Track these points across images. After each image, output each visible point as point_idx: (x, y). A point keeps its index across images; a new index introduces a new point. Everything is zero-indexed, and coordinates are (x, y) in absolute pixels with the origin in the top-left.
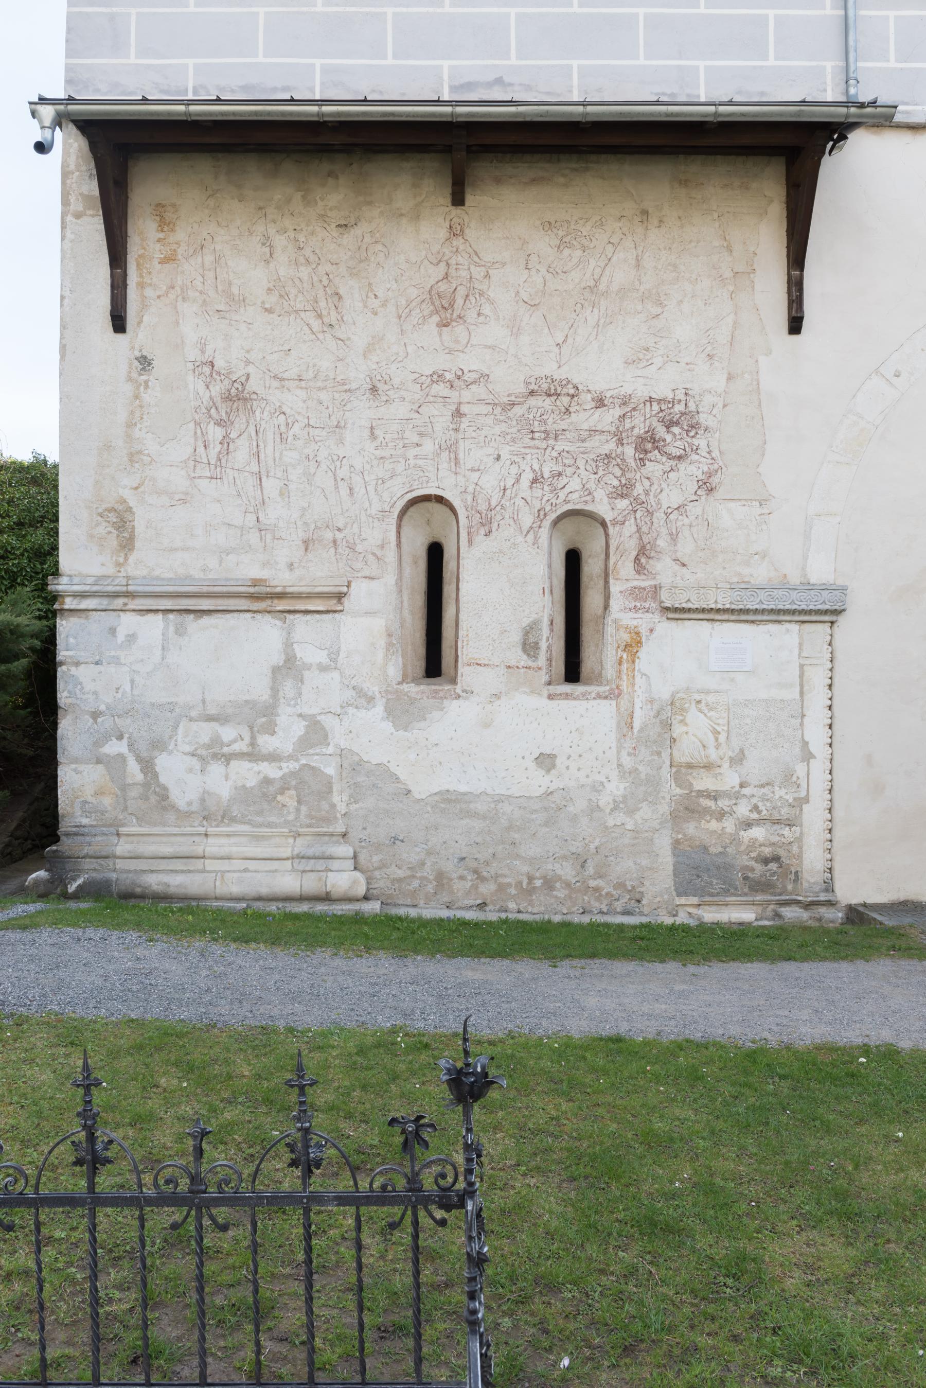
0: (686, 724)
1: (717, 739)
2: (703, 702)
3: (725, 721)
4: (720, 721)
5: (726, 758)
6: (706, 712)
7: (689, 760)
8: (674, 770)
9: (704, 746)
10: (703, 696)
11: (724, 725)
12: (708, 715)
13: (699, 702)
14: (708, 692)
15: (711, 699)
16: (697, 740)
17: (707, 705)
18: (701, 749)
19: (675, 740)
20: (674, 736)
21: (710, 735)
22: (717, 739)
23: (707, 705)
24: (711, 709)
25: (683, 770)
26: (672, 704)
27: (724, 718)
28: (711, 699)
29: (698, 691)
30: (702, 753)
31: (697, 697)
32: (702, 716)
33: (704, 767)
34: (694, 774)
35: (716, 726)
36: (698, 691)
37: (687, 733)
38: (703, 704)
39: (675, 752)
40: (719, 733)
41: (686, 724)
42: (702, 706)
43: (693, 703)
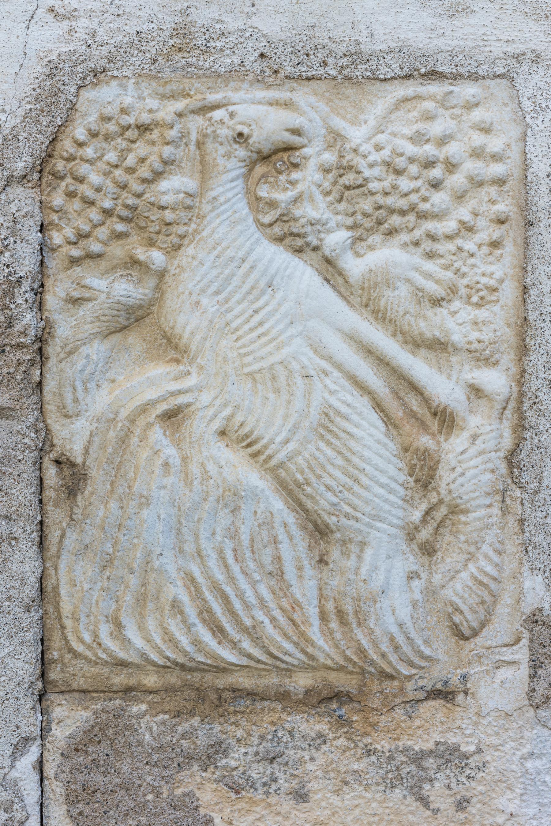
0: (171, 347)
1: (423, 472)
2: (317, 155)
3: (495, 322)
4: (457, 323)
5: (504, 624)
6: (336, 239)
7: (194, 639)
8: (70, 719)
9: (319, 531)
10: (310, 110)
11: (485, 360)
12: (355, 266)
13: (276, 157)
14: (350, 71)
15: (376, 128)
16: (254, 478)
17: (346, 183)
18: (294, 548)
19: (75, 478)
20: (73, 436)
21: (368, 432)
22: (423, 472)
23: (346, 183)
24: (377, 224)
25: (149, 724)
26: (43, 170)
27: (483, 297)
28: (376, 128)
29: (276, 69)
30: (305, 589)
31: (260, 113)
32: (303, 275)
33: (325, 699)
34: (236, 757)
35: (419, 367)
36: (276, 69)
37: (173, 417)
38: (309, 177)
39: (75, 577)
40: (445, 420)
41: (171, 347)
42: (306, 189)
43: (229, 167)
